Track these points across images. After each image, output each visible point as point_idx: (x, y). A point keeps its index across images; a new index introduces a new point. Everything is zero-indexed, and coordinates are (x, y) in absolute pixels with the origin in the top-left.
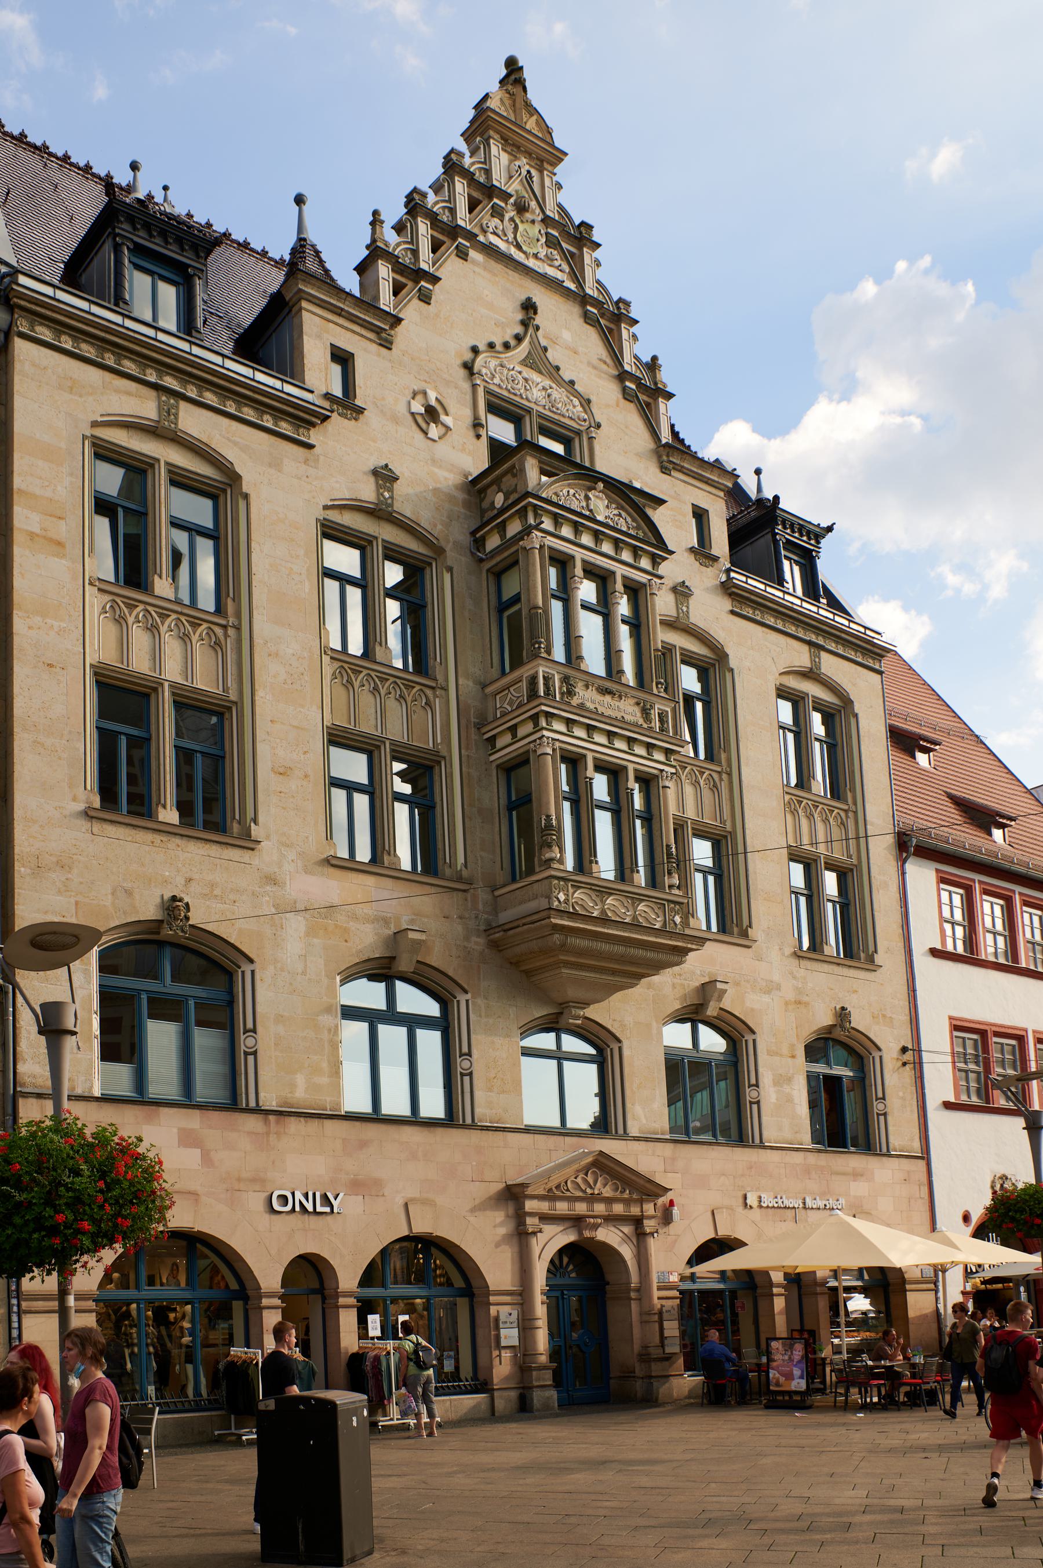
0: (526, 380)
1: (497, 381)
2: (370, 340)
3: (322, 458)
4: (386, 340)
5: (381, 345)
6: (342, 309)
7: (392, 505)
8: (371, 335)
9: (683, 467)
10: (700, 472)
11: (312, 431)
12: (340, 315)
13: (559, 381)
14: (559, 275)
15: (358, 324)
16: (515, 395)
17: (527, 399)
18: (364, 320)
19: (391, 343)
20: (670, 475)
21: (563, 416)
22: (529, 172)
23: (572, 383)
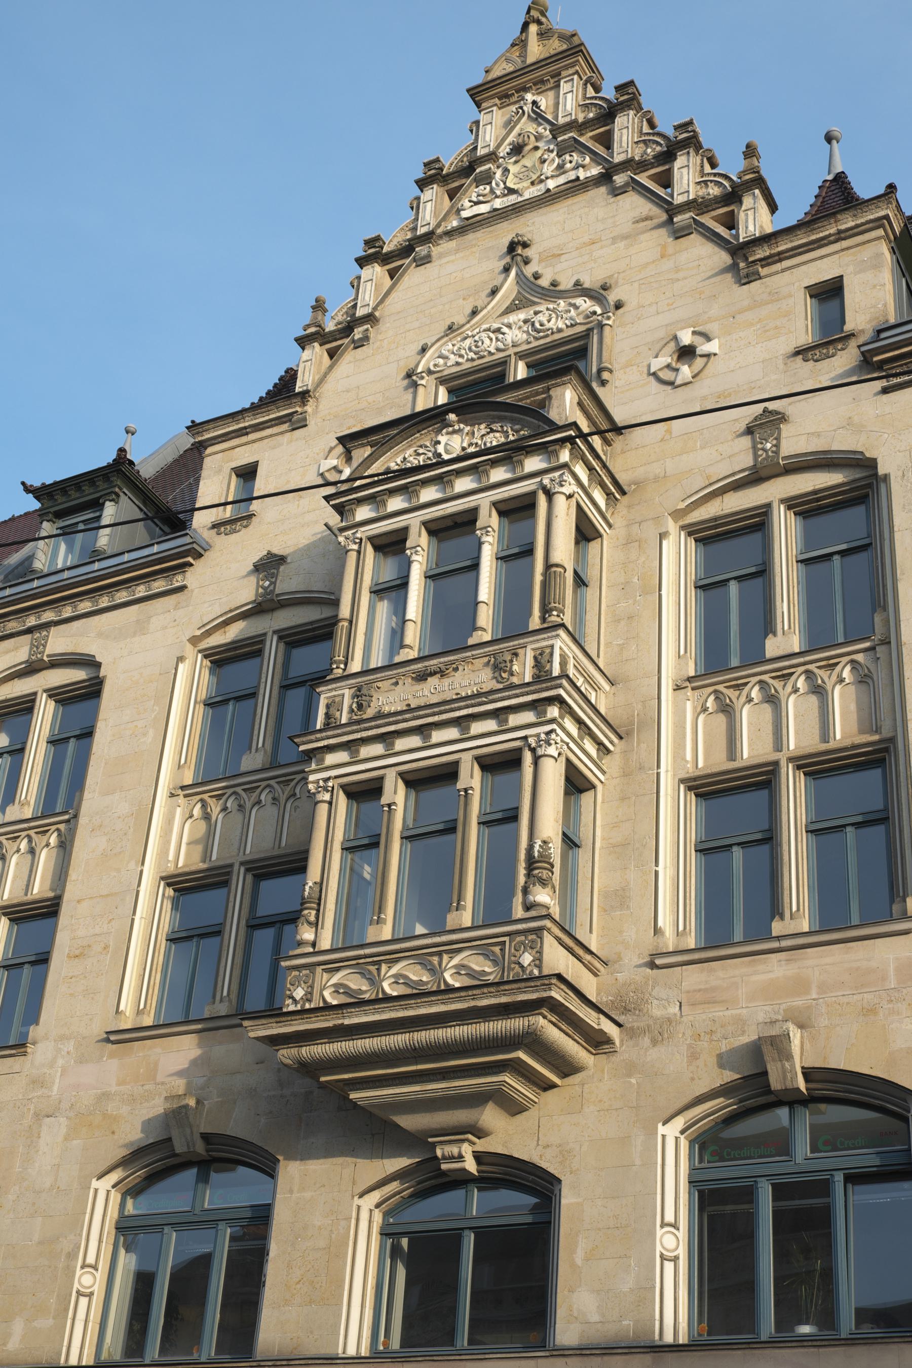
0: (498, 330)
1: (453, 359)
2: (282, 433)
3: (196, 591)
4: (299, 421)
5: (294, 429)
6: (245, 428)
7: (273, 591)
8: (285, 427)
9: (780, 253)
10: (813, 237)
11: (190, 572)
12: (247, 434)
13: (563, 295)
14: (572, 175)
15: (268, 427)
16: (483, 357)
17: (498, 350)
18: (271, 420)
19: (305, 419)
20: (760, 278)
21: (560, 330)
22: (534, 103)
23: (577, 283)
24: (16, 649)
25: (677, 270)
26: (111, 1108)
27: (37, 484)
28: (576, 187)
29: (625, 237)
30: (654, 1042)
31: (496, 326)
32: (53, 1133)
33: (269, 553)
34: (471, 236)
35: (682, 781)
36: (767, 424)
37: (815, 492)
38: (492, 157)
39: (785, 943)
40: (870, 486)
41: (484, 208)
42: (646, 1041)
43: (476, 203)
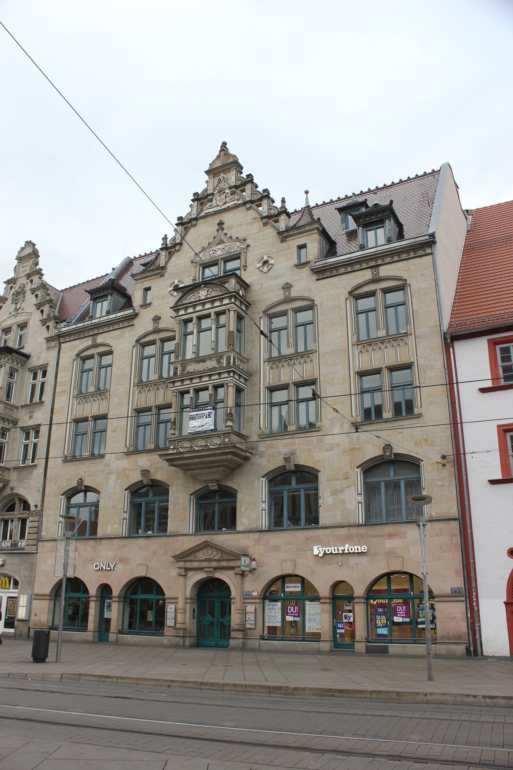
24: (88, 341)
25: (264, 236)
26: (127, 472)
27: (88, 289)
28: (237, 206)
29: (250, 224)
30: (260, 457)
31: (215, 249)
32: (113, 477)
33: (156, 316)
34: (207, 219)
35: (266, 387)
36: (287, 287)
37: (299, 307)
38: (213, 194)
39: (290, 433)
40: (313, 306)
41: (211, 210)
42: (258, 457)
43: (208, 208)
